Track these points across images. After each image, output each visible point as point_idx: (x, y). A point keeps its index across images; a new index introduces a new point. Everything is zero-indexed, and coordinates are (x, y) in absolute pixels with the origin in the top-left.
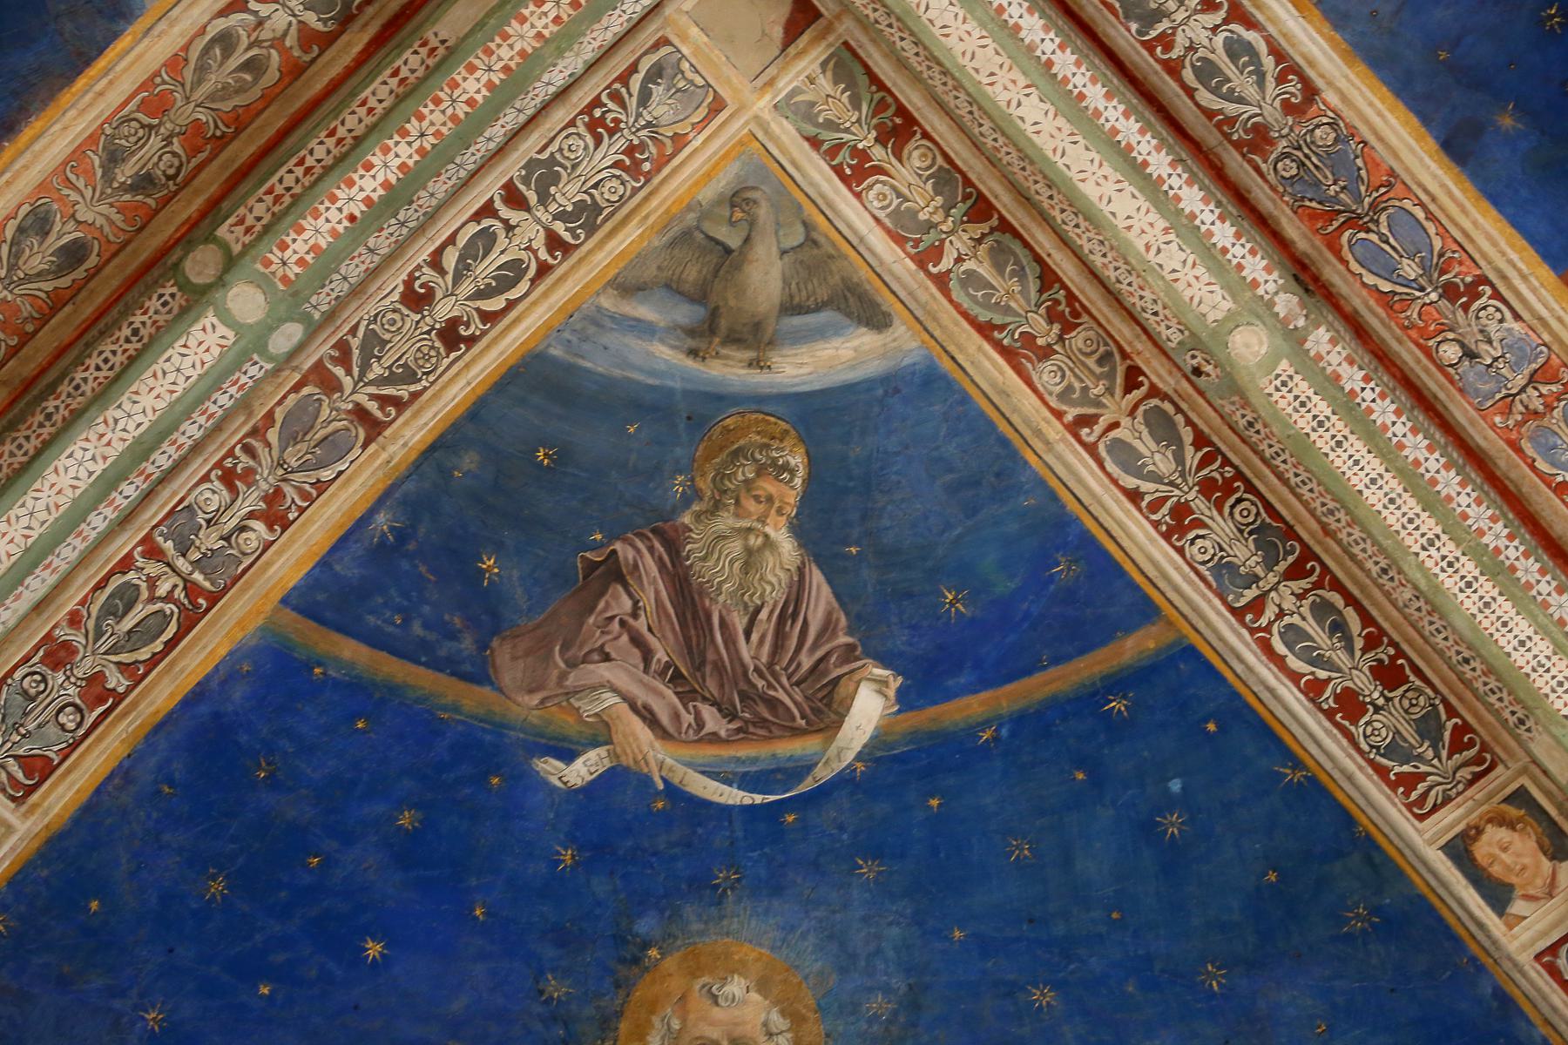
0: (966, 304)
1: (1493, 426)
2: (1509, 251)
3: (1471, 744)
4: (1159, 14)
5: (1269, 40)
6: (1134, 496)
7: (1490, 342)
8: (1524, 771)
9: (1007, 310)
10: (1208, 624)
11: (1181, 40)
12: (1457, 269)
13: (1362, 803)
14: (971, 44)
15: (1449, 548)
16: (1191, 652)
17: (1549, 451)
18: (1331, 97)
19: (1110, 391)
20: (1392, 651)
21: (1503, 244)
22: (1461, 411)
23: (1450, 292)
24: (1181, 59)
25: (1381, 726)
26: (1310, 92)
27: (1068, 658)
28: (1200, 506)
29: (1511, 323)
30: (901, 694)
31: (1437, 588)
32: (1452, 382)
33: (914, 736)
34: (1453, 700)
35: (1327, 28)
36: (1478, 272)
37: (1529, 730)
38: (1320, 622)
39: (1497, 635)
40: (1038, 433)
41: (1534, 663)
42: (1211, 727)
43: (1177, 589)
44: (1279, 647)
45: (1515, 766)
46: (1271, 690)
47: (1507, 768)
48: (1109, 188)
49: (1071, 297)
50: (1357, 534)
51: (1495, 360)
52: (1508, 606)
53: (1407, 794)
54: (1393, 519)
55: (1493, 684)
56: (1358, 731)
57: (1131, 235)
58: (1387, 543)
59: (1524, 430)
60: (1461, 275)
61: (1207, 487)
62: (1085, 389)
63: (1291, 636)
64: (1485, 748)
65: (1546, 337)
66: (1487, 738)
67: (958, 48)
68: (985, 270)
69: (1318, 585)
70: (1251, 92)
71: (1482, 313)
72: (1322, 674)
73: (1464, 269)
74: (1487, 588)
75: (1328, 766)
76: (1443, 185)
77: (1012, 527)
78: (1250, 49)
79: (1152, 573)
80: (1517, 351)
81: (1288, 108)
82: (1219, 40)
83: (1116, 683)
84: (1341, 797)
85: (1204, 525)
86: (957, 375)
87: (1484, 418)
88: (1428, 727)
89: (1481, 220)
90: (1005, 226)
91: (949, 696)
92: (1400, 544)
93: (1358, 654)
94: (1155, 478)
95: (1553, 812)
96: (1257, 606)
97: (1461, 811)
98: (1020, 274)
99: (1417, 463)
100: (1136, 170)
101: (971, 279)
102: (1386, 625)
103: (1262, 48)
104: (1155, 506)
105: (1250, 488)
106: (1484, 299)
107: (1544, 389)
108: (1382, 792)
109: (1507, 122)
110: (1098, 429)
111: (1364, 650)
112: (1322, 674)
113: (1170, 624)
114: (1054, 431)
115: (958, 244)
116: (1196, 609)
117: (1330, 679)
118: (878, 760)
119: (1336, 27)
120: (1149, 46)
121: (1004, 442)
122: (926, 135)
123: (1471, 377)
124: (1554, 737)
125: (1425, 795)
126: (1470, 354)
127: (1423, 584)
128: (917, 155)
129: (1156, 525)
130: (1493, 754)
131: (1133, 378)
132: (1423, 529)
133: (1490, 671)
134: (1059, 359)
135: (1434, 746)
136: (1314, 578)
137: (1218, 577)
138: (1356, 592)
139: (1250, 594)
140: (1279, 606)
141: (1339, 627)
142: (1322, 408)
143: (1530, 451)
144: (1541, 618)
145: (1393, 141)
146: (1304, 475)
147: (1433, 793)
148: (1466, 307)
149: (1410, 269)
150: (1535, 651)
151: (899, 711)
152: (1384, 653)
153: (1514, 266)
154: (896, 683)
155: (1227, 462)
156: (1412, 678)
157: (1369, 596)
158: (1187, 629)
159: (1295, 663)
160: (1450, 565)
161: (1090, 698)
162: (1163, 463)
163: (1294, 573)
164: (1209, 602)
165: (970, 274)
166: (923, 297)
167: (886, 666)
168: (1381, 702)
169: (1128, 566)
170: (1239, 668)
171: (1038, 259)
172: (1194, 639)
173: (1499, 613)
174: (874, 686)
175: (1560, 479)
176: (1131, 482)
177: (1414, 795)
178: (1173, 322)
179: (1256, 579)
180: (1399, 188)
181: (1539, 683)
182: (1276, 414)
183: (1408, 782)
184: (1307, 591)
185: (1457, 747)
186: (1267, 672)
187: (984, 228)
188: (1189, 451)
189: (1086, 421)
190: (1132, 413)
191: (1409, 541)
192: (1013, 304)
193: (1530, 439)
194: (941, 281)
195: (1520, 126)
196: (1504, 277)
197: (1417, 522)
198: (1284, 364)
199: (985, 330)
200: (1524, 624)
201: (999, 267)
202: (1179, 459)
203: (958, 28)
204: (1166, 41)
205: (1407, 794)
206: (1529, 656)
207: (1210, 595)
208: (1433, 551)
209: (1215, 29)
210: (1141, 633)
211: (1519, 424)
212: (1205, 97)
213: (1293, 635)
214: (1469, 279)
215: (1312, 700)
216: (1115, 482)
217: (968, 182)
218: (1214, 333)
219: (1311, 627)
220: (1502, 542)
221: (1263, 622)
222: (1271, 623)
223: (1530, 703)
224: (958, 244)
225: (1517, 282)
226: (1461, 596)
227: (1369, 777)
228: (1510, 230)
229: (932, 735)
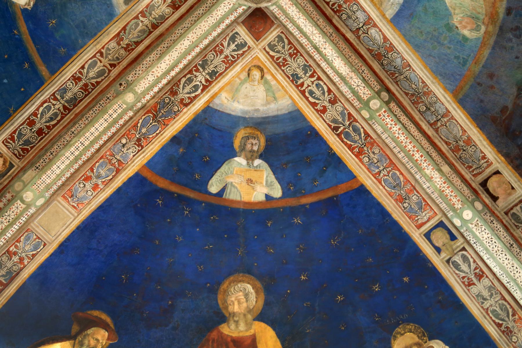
0: (131, 24)
1: (106, 152)
2: (150, 153)
3: (24, 153)
4: (204, 69)
5: (199, 95)
6: (83, 67)
7: (127, 150)
8: (19, 166)
9: (129, 34)
10: (50, 87)
11: (198, 74)
12: (145, 141)
13: (6, 128)
14: (203, 28)
15: (81, 148)
16: (42, 83)
17: (101, 165)
18: (185, 110)
19: (110, 60)
20: (46, 132)
21: (152, 151)
22: (109, 145)
23: (139, 140)
24: (193, 74)
25: (28, 133)
26: (186, 105)
27: (39, 52)
28: (81, 84)
29: (132, 154)
30: (26, 9)
31: (71, 146)
32: (117, 142)
33: (14, 13)
34: (35, 148)
35: (202, 108)
36: (144, 146)
37: (35, 170)
38: (52, 115)
39: (60, 161)
40: (98, 43)
41: (54, 170)
42: (22, 89)
43: (59, 79)
44: (45, 105)
45: (20, 164)
46: (33, 104)
47: (19, 162)
48: (168, 62)
49: (133, 49)
50: (83, 126)
51: (123, 152)
52: (68, 163)
53: (9, 138)
54: (87, 134)
55: (47, 161)
56: (25, 125)
57: (156, 68)
58: (81, 133)
59: (106, 159)
60: (143, 142)
61: (86, 85)
62: (110, 54)
63: (49, 108)
64: (23, 156)
65: (129, 163)
66: (26, 157)
67: (202, 25)
68: (139, 28)
69: (62, 113)
70: (186, 91)
71: (134, 148)
72: (39, 116)
73: (145, 143)
74: (72, 158)
75: (15, 119)
76: (165, 137)
77: (73, 37)
78: (196, 90)
79: (63, 73)
80: (125, 156)
81: (182, 100)
82: (198, 83)
83: (32, 65)
84: (7, 122)
85: (76, 85)
86: (113, 22)
87: (108, 150)
88: (27, 142)
89: (157, 146)
90: (150, 33)
91: (26, 22)
92: (81, 136)
93: (45, 124)
94: (88, 72)
95: (9, 174)
96: (56, 99)
97: (6, 152)
98: (138, 37)
99: (102, 138)
100: (172, 69)
101: (137, 25)
102: (53, 130)
103: (197, 93)
104: (81, 73)
105: (86, 96)
106: (137, 148)
107: (116, 163)
108: (9, 132)
109: (181, 150)
110: (100, 58)
111: (46, 126)
112: (39, 116)
113: (50, 78)
114: (99, 47)
115: (146, 21)
116: (54, 84)
117: (38, 118)
118: (7, 3)
119: (203, 110)
120: (196, 66)
121: (95, 34)
122: (173, 13)
123: (118, 146)
124: (35, 177)
125: (9, 143)
126: (124, 146)
127: (71, 143)
128: (168, 10)
129: (76, 73)
130: (22, 158)
131: (113, 66)
132: (86, 142)
133: (50, 160)
134: (117, 47)
135: (22, 144)
136: (64, 112)
137: (63, 89)
138: (61, 122)
139: (59, 97)
140: (56, 104)
141: (51, 119)
142: (115, 116)
143: (101, 161)
144: (65, 171)
145: (175, 125)
146: (96, 112)
147: (10, 145)
148: (135, 144)
149: (144, 130)
150: (57, 170)
151: (21, 9)
152: (46, 131)
153: (146, 154)
154: (29, 8)
155: (93, 90)
156: (40, 138)
157: (60, 126)
158: (49, 82)
159: (41, 109)
160: (77, 149)
161: (28, 59)
162: (91, 74)
163: (65, 107)
164: (56, 87)
165: (138, 24)
166: (133, 13)
167: (34, 5)
168: (33, 131)
169: (64, 67)
170: (39, 96)
171: (142, 41)
172: (46, 84)
173: (66, 161)
174: (28, 2)
175: (94, 168)
176: (86, 66)
177: (9, 140)
178: (133, 79)
179: (63, 98)
180: (164, 127)
181: (49, 172)
182: (112, 105)
183: (12, 139)
184: (60, 111)
185: (23, 150)
186: (38, 102)
187: (150, 28)
188: (95, 80)
189: (102, 55)
190: (104, 66)
191: (82, 139)
192: (131, 35)
193: (104, 161)
194: (137, 17)
195: (180, 153)
196: (143, 152)
197: (87, 140)
198: (125, 106)
199: (124, 29)
200: (63, 167)
201: (140, 31)
202: (93, 78)
203: (207, 24)
204: (197, 70)
205: (9, 138)
206: (55, 169)
207: (58, 87)
208: (80, 144)
209: (201, 82)
210: (46, 70)
211: (107, 158)
212: (184, 80)
213: (49, 108)
214: (142, 144)
215: (32, 114)
216: (86, 62)
217: (162, 23)
218: (132, 89)
219: (51, 112)
220: (82, 160)
221: (52, 101)
222: (51, 102)
223: (43, 170)
224: (146, 21)
225: (143, 155)
226: (69, 152)
227: (13, 129)
228: (155, 153)
229: (15, 18)
